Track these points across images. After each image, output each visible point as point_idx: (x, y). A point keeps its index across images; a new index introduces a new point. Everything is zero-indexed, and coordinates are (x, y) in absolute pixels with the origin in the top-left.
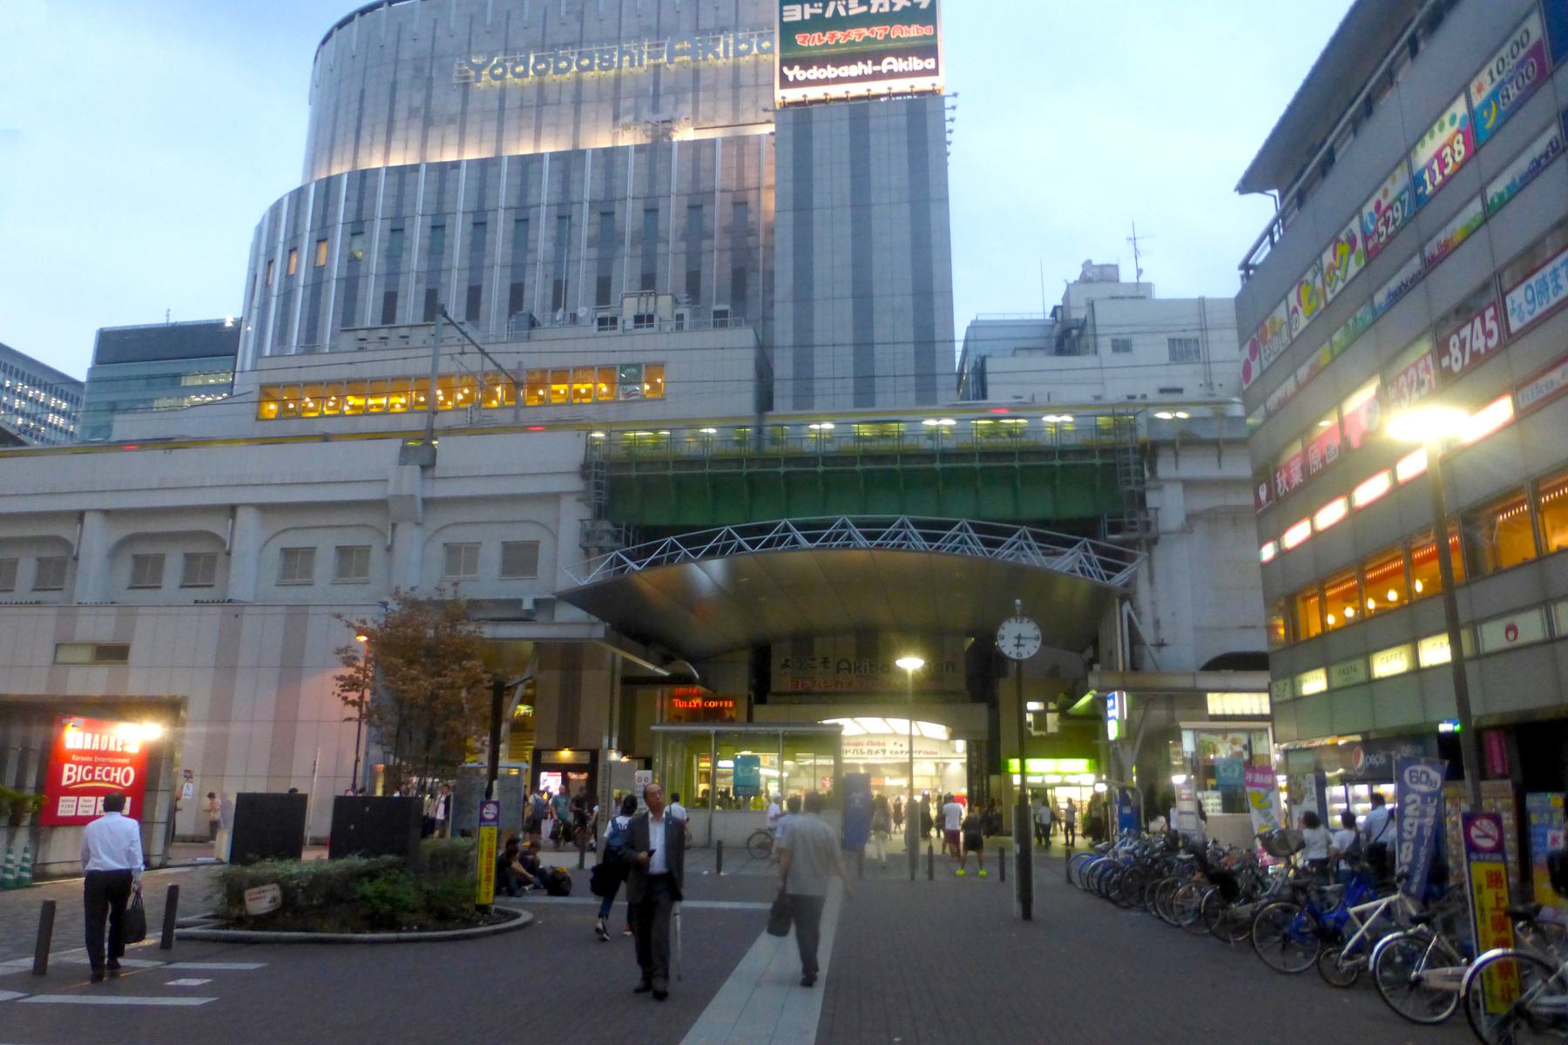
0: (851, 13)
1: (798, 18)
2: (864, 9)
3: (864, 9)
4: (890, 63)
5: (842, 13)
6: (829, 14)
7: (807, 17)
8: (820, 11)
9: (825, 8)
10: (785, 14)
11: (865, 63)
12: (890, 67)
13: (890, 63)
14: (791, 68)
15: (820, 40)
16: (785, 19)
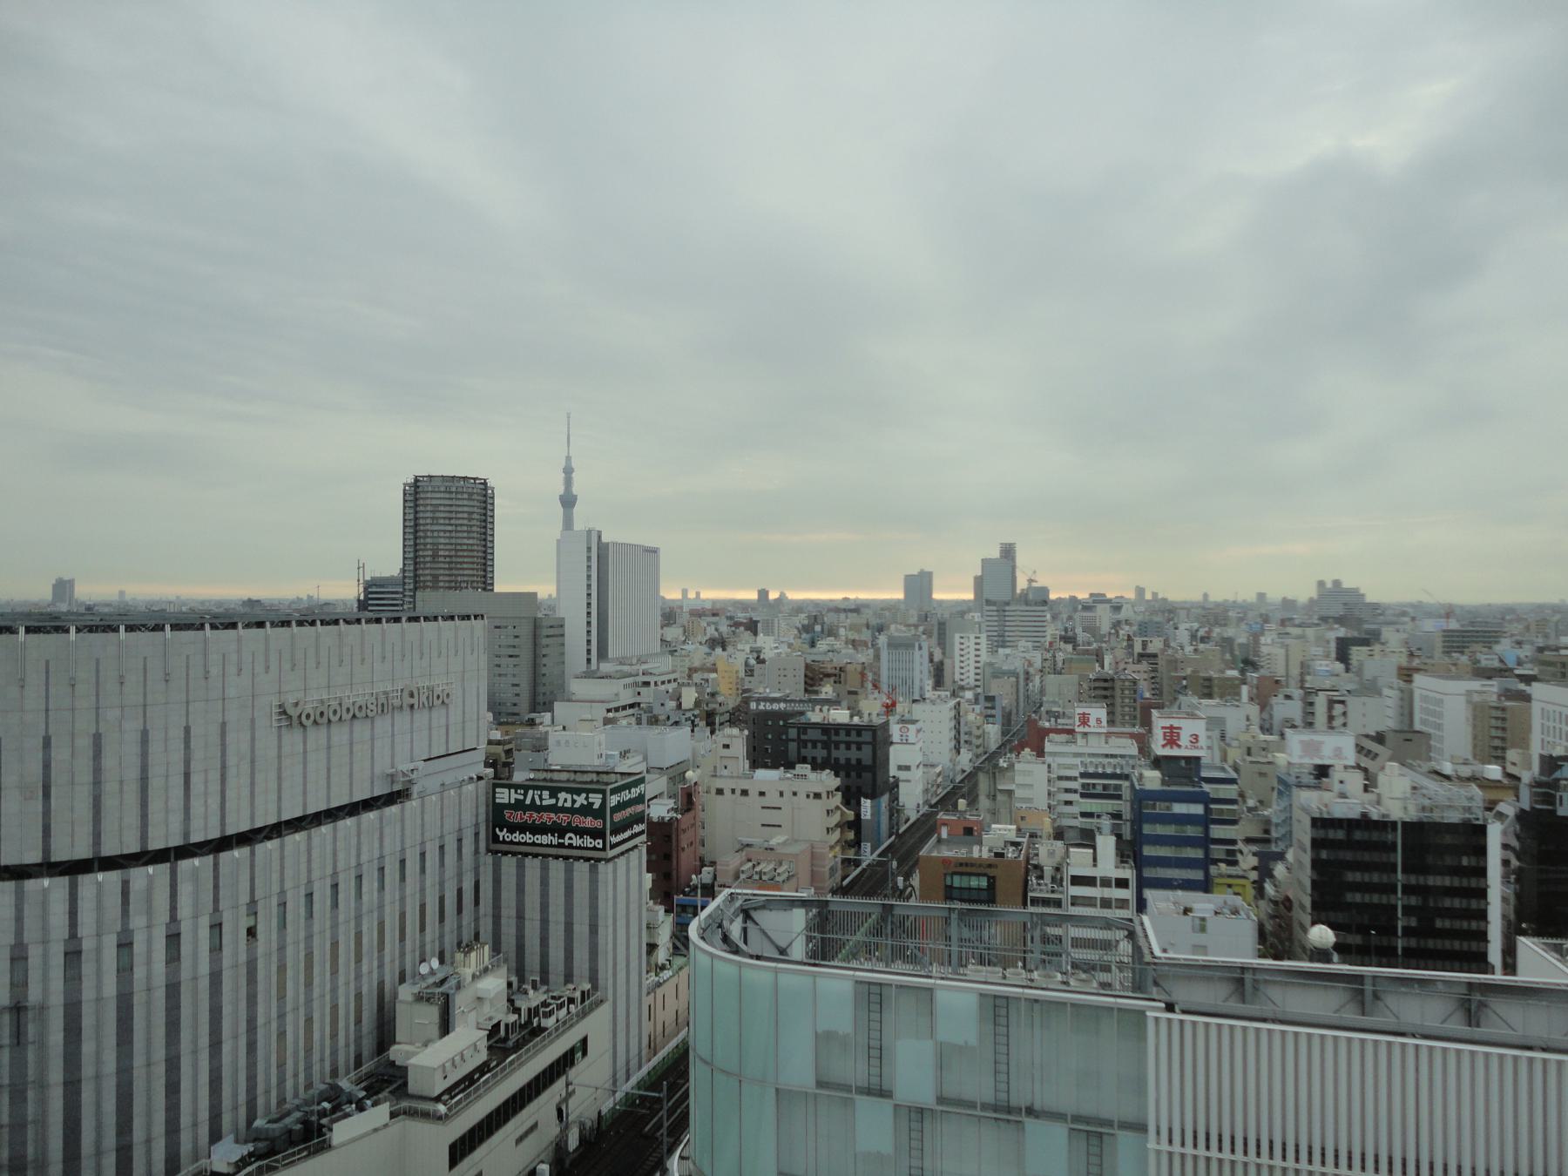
0: (544, 803)
1: (507, 802)
2: (553, 801)
3: (553, 801)
4: (570, 838)
5: (538, 803)
6: (528, 802)
7: (513, 801)
8: (522, 797)
9: (525, 795)
10: (497, 795)
11: (553, 835)
12: (570, 841)
13: (570, 838)
14: (501, 830)
15: (521, 819)
16: (498, 801)
